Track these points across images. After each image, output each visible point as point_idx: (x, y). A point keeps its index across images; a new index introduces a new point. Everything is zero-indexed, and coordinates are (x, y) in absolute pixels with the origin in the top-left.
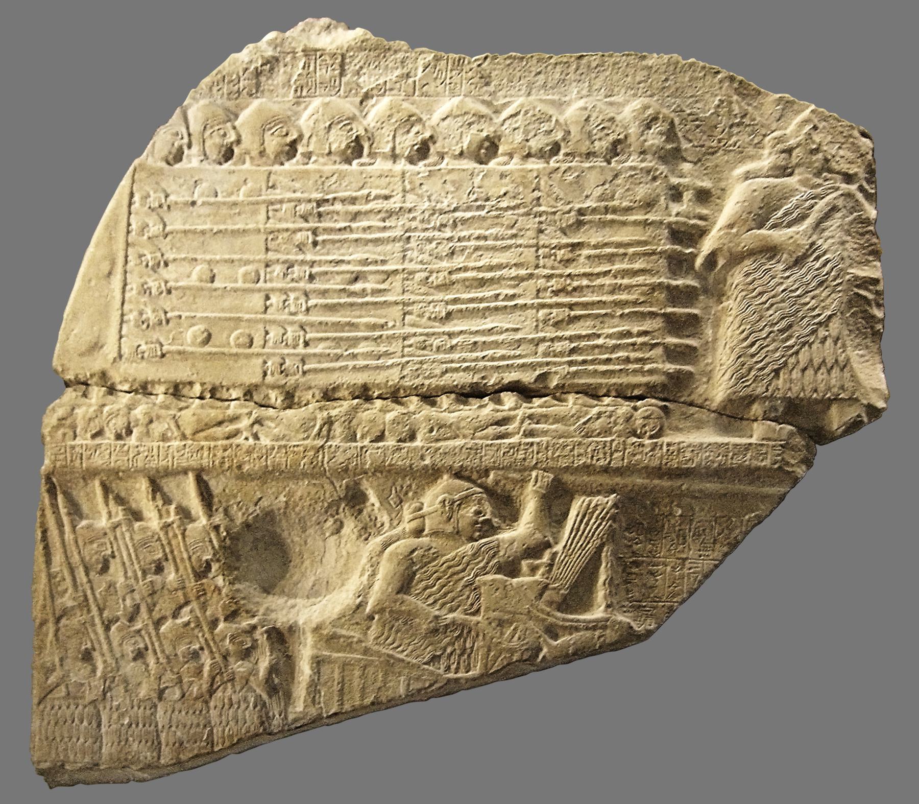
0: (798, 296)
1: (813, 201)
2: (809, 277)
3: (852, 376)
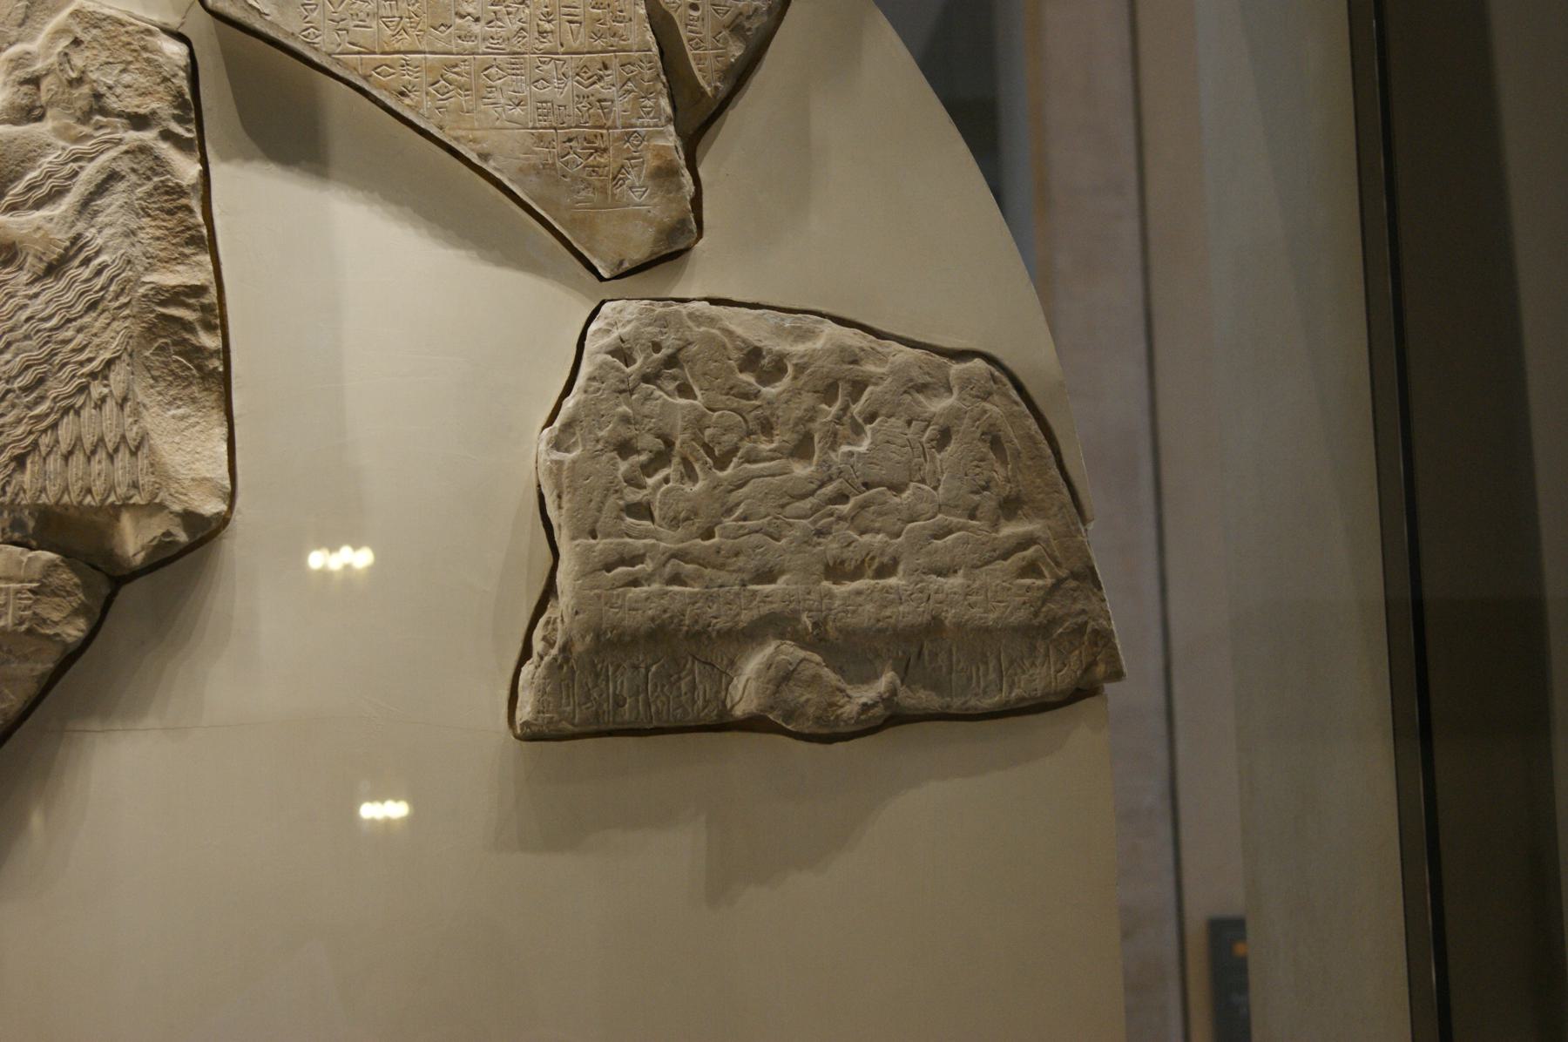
0: (51, 330)
1: (75, 166)
2: (71, 295)
3: (152, 465)
